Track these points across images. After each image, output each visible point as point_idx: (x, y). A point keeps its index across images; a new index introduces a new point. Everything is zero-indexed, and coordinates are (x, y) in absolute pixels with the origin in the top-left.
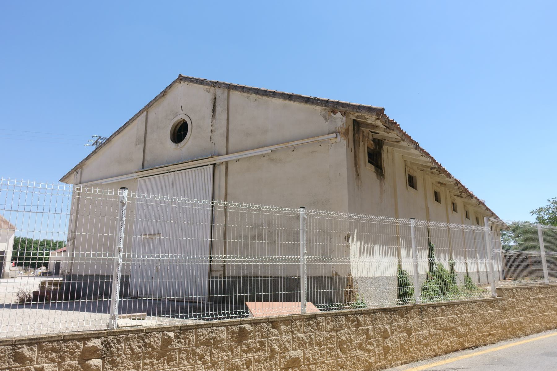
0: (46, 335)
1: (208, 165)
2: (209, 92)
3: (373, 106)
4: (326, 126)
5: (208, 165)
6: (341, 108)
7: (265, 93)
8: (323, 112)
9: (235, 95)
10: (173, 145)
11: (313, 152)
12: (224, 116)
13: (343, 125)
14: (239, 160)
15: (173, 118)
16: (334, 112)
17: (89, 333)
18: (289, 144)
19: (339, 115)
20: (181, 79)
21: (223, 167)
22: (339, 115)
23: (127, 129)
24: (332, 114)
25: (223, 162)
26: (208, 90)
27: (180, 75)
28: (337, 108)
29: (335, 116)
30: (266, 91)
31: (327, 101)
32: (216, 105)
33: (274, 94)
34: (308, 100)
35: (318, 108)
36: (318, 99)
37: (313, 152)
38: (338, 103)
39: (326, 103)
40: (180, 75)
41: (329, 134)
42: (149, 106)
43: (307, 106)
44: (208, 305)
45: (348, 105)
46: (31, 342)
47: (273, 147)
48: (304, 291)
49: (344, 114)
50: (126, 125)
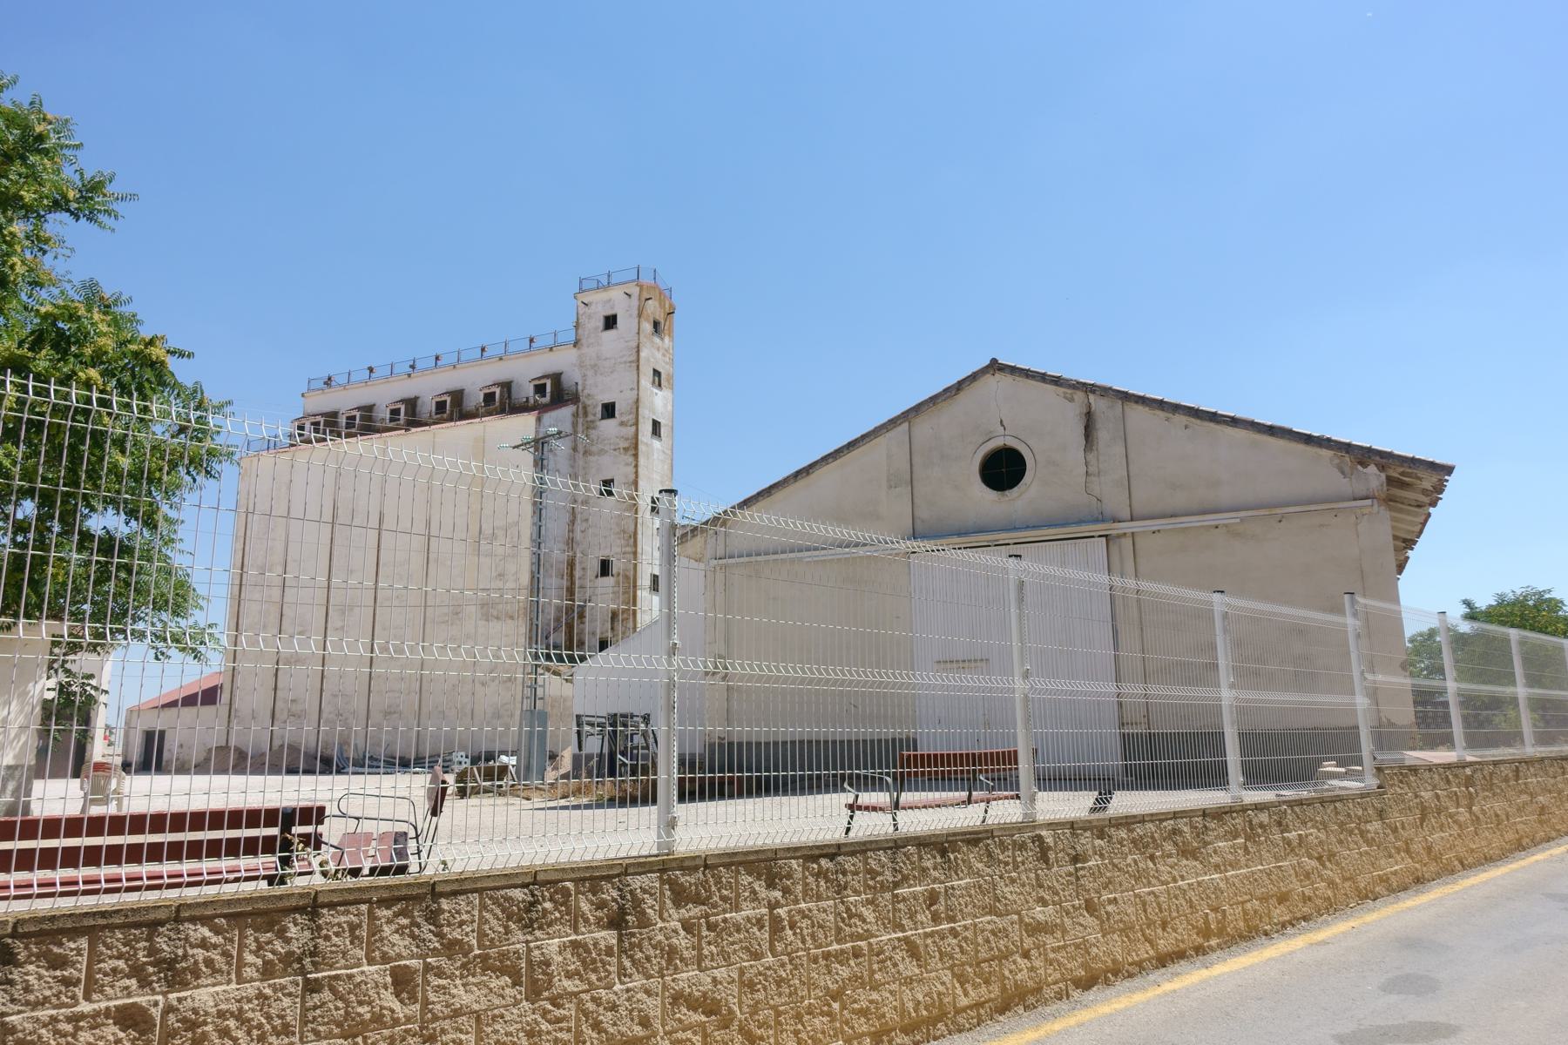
0: (602, 861)
1: (1093, 537)
2: (1072, 400)
3: (1438, 461)
4: (1344, 485)
5: (1093, 537)
6: (1378, 458)
7: (1213, 417)
8: (1337, 461)
9: (1137, 413)
10: (990, 495)
11: (1321, 525)
12: (1119, 449)
13: (1382, 485)
14: (1159, 531)
15: (981, 441)
16: (1364, 464)
17: (627, 861)
18: (1278, 511)
19: (1372, 469)
20: (995, 367)
21: (1127, 542)
22: (1372, 469)
23: (855, 453)
24: (1359, 467)
25: (1125, 534)
26: (1068, 396)
27: (994, 361)
28: (1370, 458)
29: (1365, 470)
30: (1215, 414)
31: (1349, 446)
32: (1097, 427)
33: (1234, 422)
34: (1308, 439)
35: (1326, 453)
36: (1329, 440)
37: (1321, 525)
38: (1370, 450)
39: (1347, 448)
40: (994, 361)
41: (1355, 499)
42: (917, 409)
43: (1301, 447)
44: (1123, 781)
45: (1390, 455)
46: (793, 851)
47: (1243, 514)
48: (1233, 758)
49: (1382, 468)
50: (852, 445)
